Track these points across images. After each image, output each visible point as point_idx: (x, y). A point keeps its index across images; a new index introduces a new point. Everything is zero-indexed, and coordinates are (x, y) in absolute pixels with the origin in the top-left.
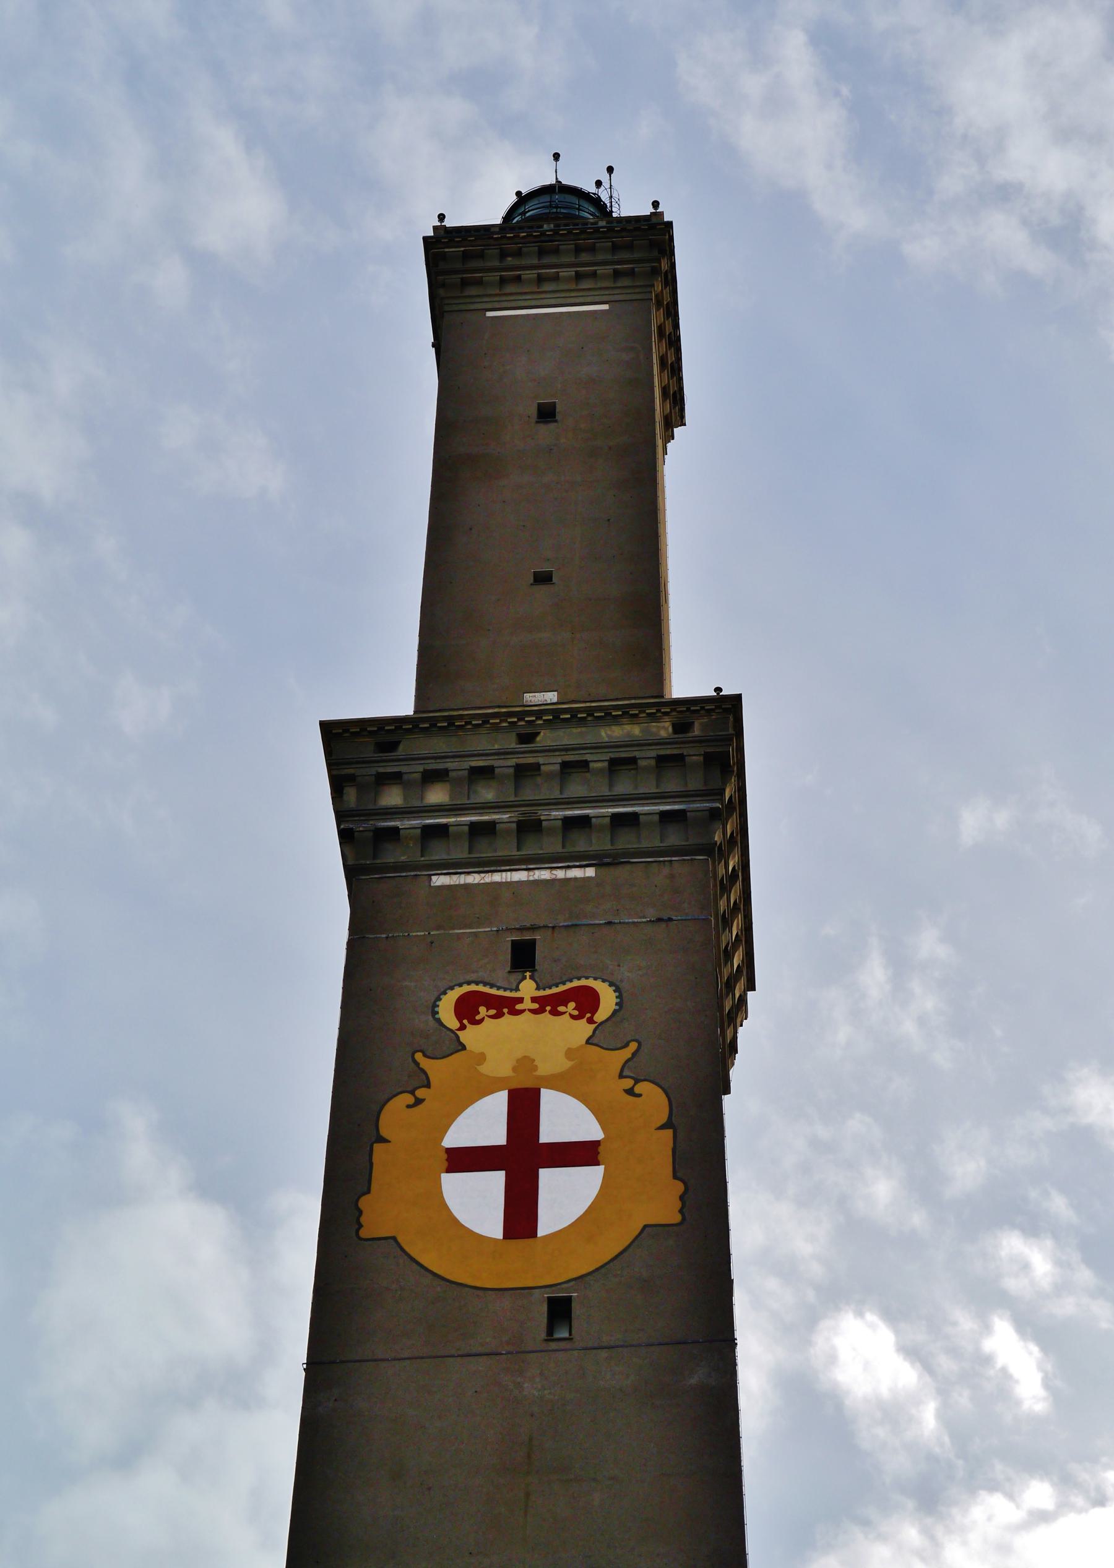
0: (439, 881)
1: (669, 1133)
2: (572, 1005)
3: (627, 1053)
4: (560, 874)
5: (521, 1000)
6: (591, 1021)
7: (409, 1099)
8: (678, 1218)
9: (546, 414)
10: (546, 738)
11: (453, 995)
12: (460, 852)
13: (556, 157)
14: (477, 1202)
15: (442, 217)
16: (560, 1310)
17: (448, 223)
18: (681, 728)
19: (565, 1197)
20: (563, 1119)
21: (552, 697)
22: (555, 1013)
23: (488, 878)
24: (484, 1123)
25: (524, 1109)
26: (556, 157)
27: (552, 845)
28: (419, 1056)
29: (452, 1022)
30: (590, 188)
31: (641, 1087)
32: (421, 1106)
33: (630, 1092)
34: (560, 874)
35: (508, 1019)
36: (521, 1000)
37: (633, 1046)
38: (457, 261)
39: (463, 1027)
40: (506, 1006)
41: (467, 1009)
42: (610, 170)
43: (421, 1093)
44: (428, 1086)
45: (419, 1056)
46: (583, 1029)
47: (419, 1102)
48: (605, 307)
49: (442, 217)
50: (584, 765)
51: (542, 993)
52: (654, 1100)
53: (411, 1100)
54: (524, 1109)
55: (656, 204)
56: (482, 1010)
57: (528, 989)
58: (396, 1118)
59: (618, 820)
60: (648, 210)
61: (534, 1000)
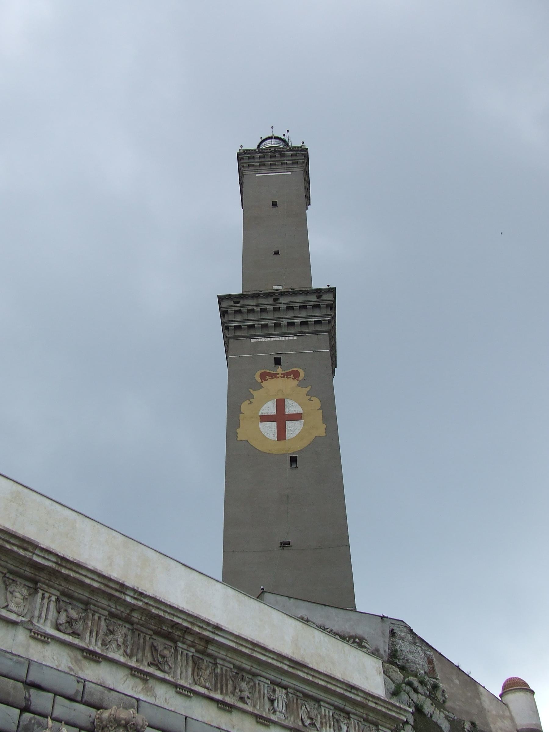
0: (253, 340)
2: (292, 375)
3: (308, 389)
5: (278, 374)
6: (297, 380)
7: (248, 402)
8: (325, 434)
9: (275, 204)
10: (282, 300)
11: (258, 373)
12: (259, 332)
13: (272, 127)
14: (270, 430)
15: (242, 146)
16: (293, 460)
17: (244, 148)
18: (319, 297)
19: (293, 428)
20: (292, 407)
21: (281, 287)
22: (287, 378)
23: (267, 340)
24: (270, 408)
25: (280, 404)
26: (272, 127)
27: (284, 330)
28: (250, 390)
29: (260, 381)
30: (282, 137)
32: (252, 404)
33: (310, 400)
34: (287, 338)
35: (275, 379)
36: (278, 374)
37: (310, 387)
38: (247, 160)
39: (262, 382)
40: (274, 376)
41: (263, 377)
42: (288, 131)
45: (250, 390)
46: (296, 382)
47: (251, 403)
48: (290, 173)
49: (242, 146)
50: (292, 308)
51: (284, 372)
52: (316, 402)
53: (249, 402)
54: (280, 404)
55: (303, 143)
56: (267, 377)
57: (279, 370)
58: (245, 407)
59: (303, 323)
60: (301, 144)
61: (281, 374)
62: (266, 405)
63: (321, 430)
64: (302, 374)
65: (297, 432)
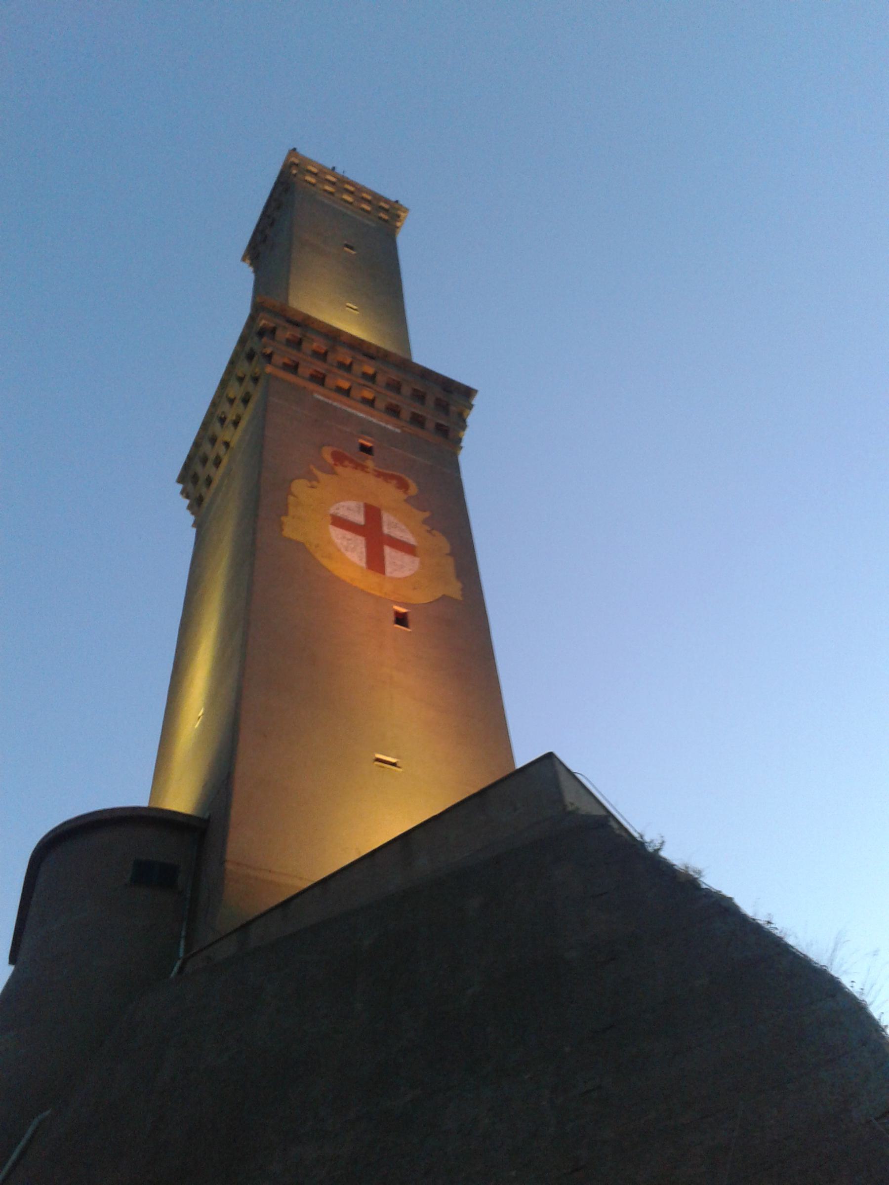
1: (451, 560)
2: (394, 482)
3: (427, 514)
4: (383, 424)
5: (367, 468)
6: (405, 492)
8: (461, 599)
19: (399, 565)
28: (312, 467)
29: (330, 460)
31: (434, 532)
35: (359, 474)
39: (336, 465)
41: (339, 458)
43: (315, 483)
44: (318, 481)
45: (312, 467)
47: (312, 487)
51: (377, 468)
54: (373, 514)
57: (370, 463)
61: (375, 471)
62: (342, 503)
63: (454, 589)
64: (413, 489)
65: (406, 573)
